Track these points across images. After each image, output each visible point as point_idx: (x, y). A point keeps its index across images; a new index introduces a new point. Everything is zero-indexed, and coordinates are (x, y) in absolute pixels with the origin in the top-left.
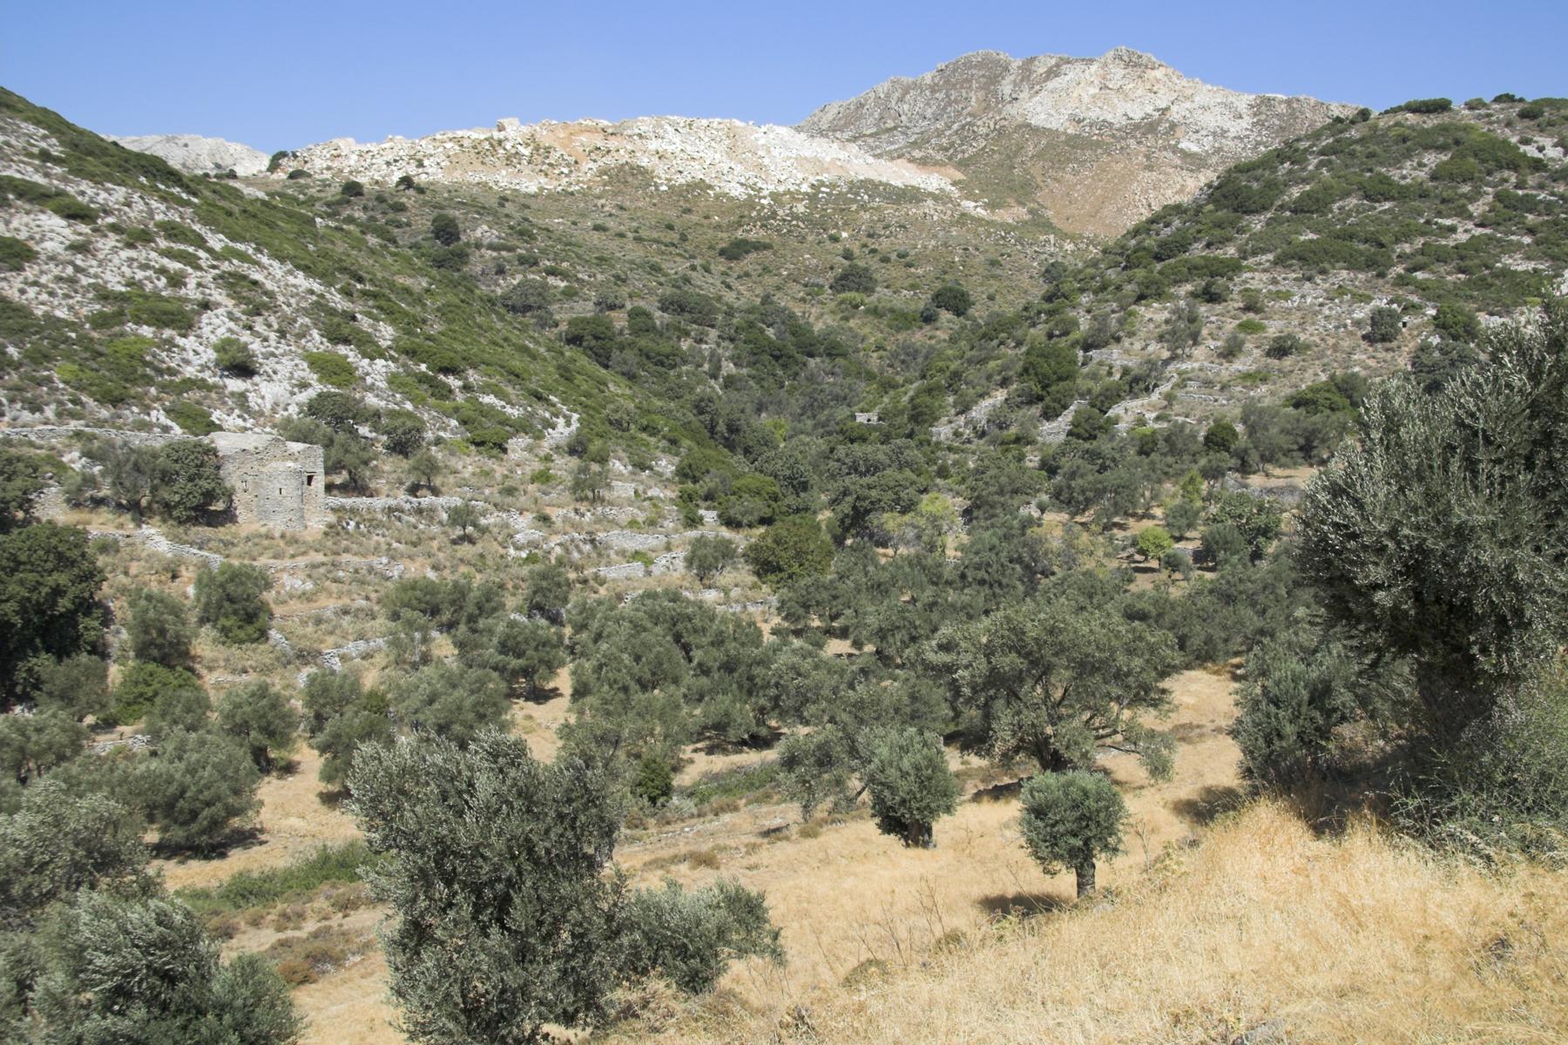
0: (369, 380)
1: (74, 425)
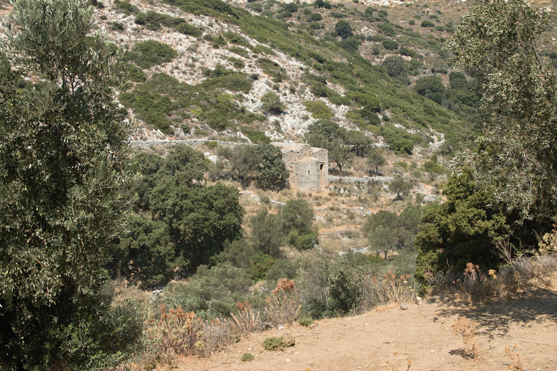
0: (337, 115)
1: (205, 139)
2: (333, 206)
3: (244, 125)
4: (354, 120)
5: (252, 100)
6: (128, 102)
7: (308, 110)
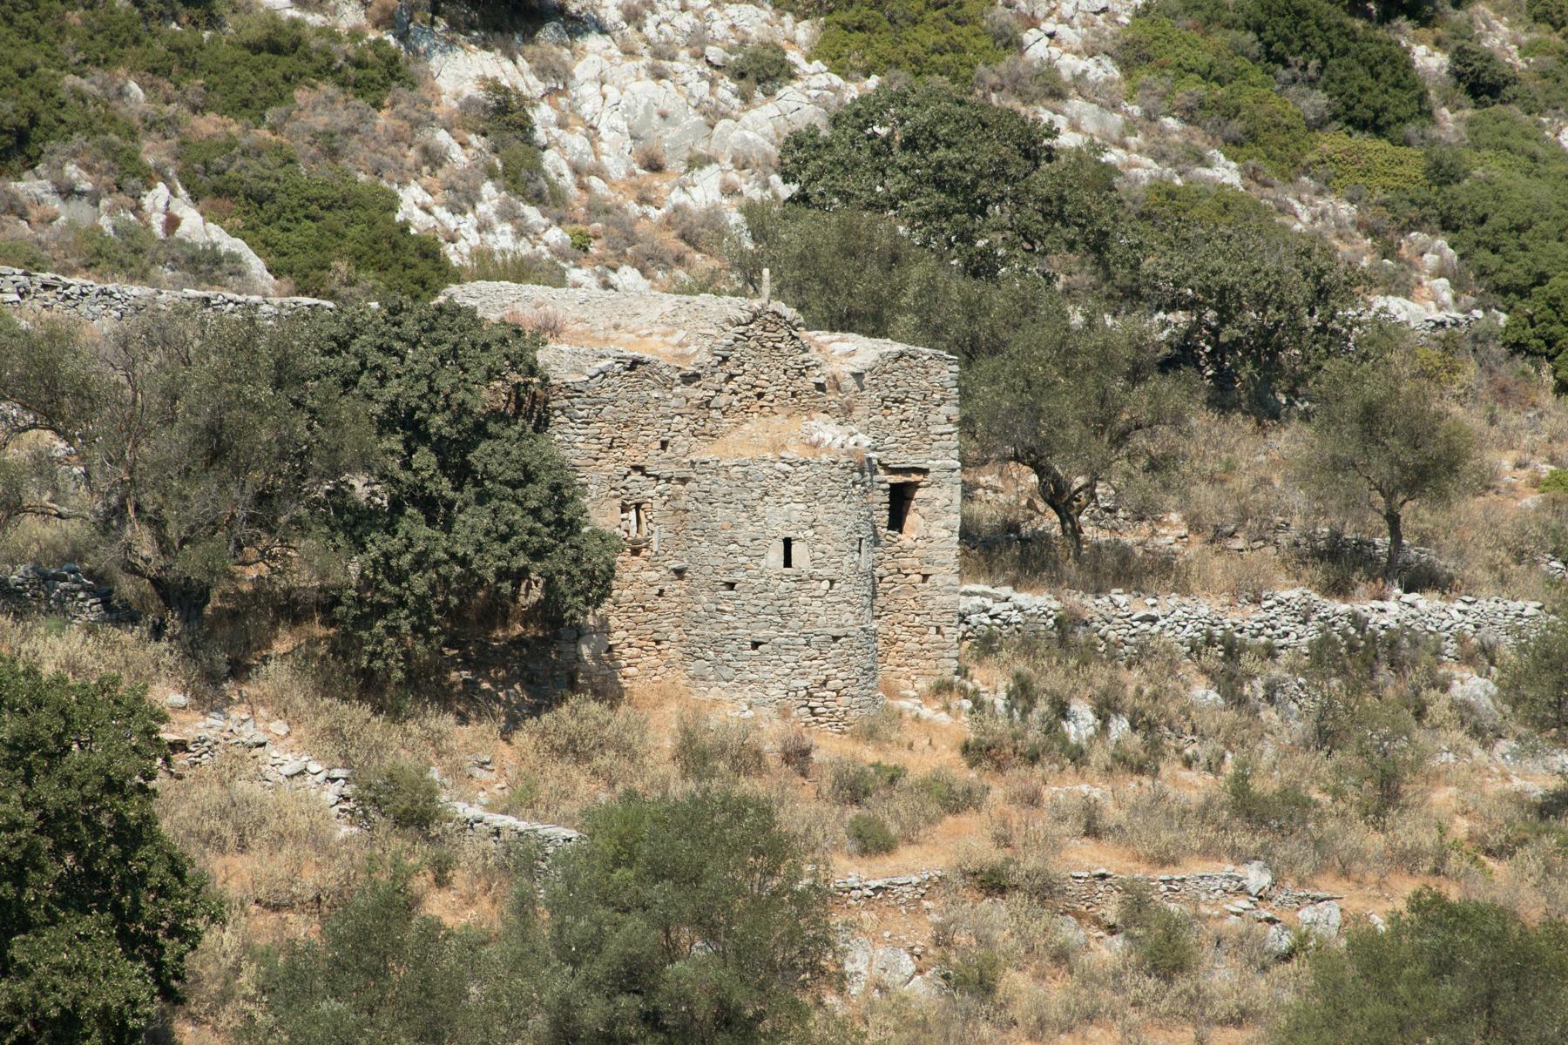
0: (1037, 48)
2: (997, 856)
3: (208, 125)
4: (1195, 88)
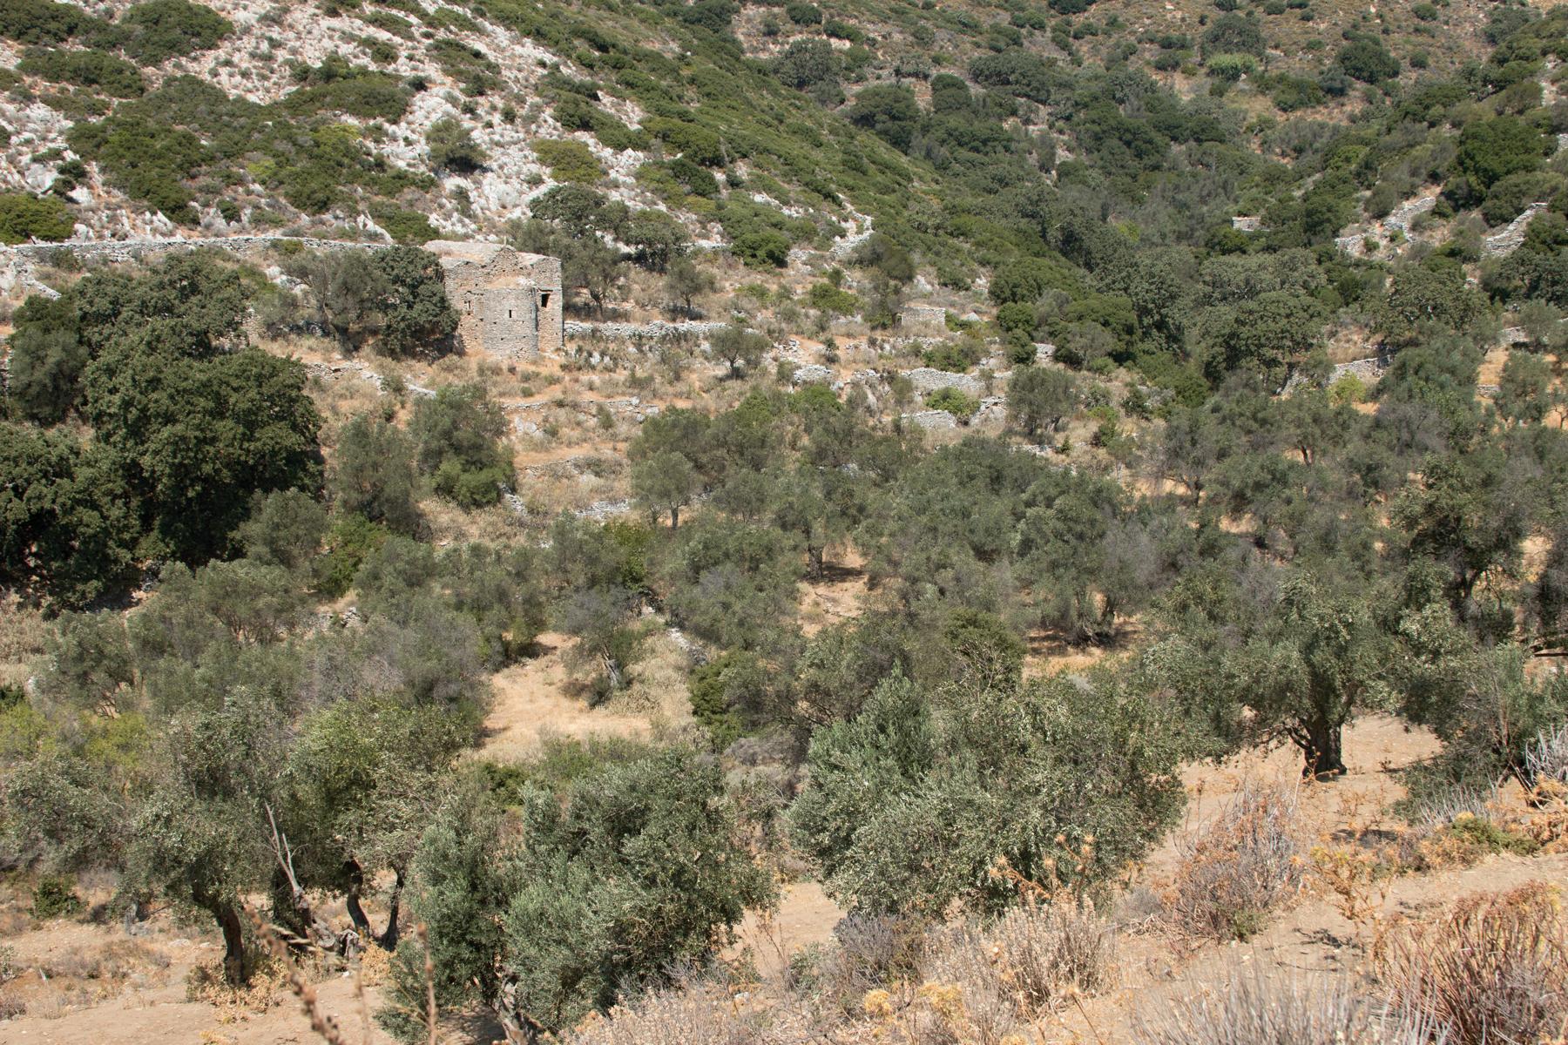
0: (613, 174)
1: (275, 234)
2: (561, 397)
3: (379, 199)
4: (654, 185)
5: (406, 139)
6: (89, 146)
7: (542, 161)
